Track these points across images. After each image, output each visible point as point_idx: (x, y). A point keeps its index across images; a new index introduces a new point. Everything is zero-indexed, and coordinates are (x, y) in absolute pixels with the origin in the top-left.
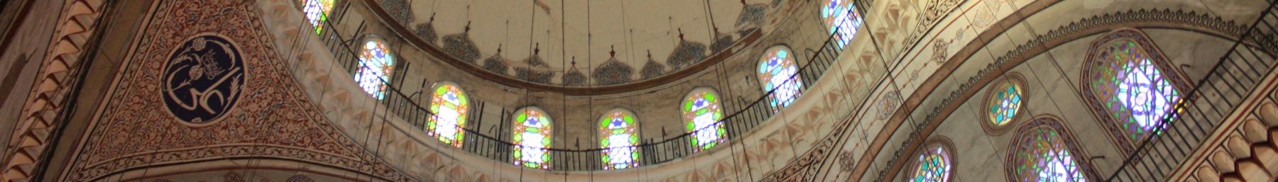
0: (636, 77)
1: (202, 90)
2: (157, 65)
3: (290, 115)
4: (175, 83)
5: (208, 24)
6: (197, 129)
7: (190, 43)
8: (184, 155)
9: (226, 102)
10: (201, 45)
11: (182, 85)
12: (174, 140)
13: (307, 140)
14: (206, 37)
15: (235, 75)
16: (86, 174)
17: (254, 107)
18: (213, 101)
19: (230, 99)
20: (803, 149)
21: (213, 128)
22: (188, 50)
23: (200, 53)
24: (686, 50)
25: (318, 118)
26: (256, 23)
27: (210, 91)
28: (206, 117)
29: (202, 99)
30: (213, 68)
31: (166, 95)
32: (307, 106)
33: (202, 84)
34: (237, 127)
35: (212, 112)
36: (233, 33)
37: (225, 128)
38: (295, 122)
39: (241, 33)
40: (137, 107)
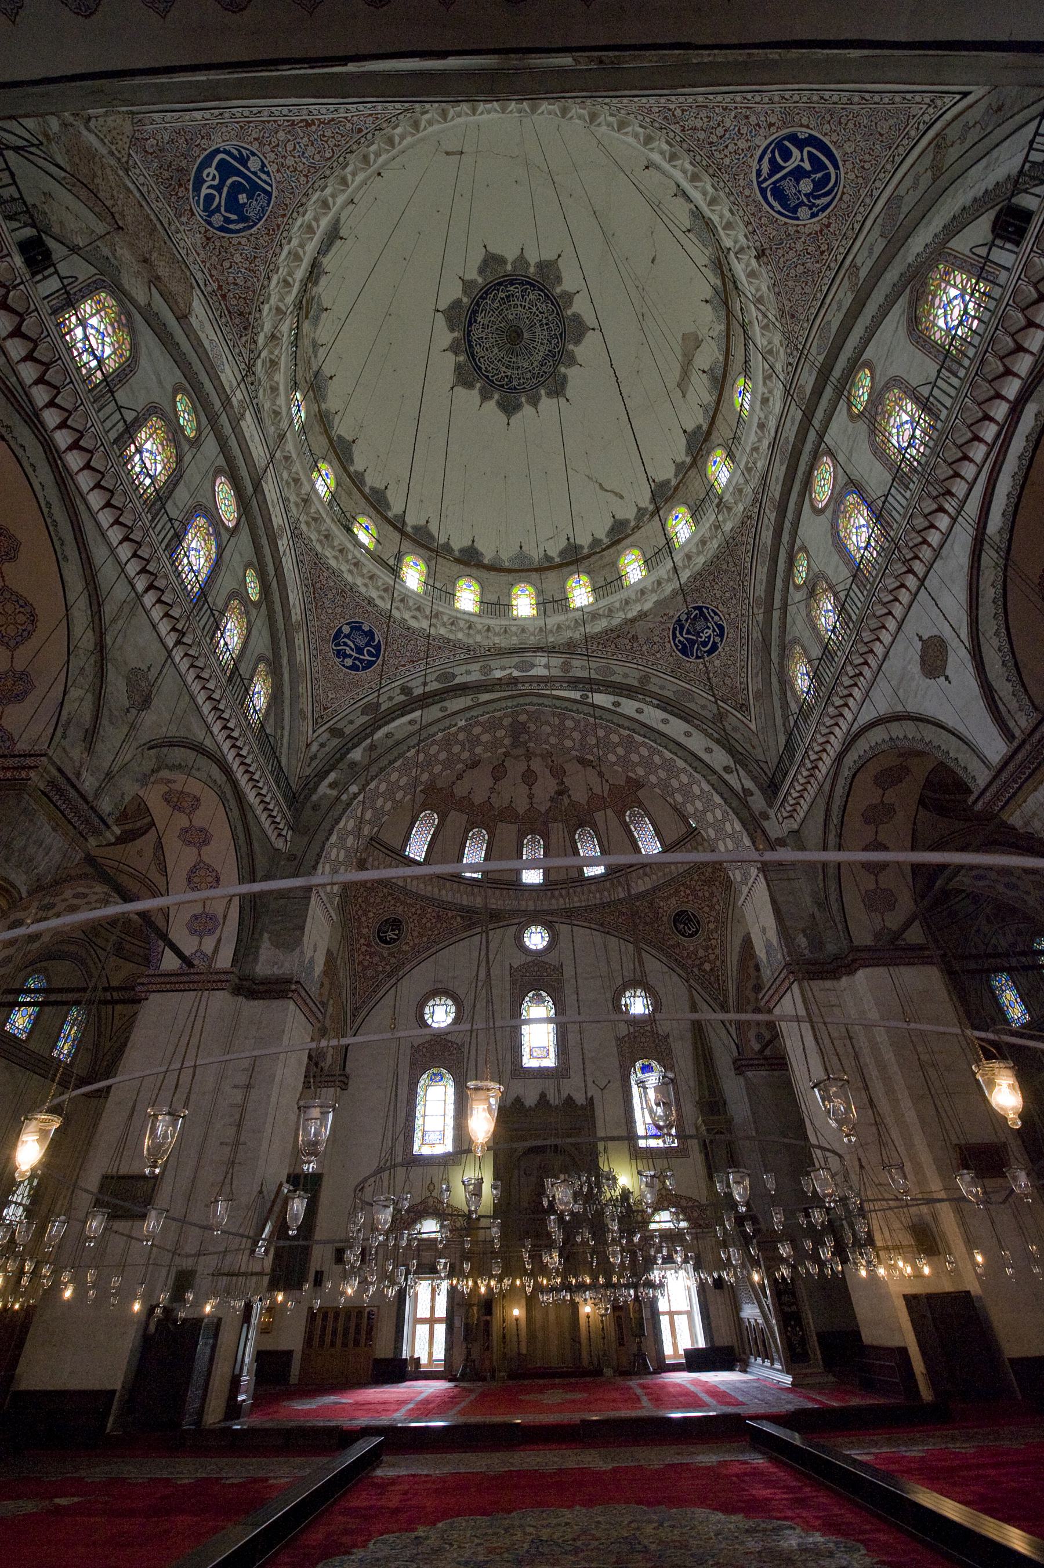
1: (799, 167)
2: (846, 198)
3: (702, 135)
4: (828, 177)
5: (797, 232)
6: (802, 126)
8: (815, 98)
9: (773, 152)
10: (803, 212)
11: (819, 175)
12: (828, 117)
13: (678, 112)
14: (798, 219)
15: (765, 180)
16: (927, 100)
17: (742, 144)
18: (787, 155)
19: (768, 155)
22: (815, 209)
25: (672, 135)
26: (751, 228)
27: (791, 165)
28: (793, 138)
29: (798, 158)
30: (789, 187)
31: (836, 167)
33: (798, 174)
34: (758, 125)
35: (786, 143)
37: (771, 125)
38: (695, 129)
40: (867, 157)
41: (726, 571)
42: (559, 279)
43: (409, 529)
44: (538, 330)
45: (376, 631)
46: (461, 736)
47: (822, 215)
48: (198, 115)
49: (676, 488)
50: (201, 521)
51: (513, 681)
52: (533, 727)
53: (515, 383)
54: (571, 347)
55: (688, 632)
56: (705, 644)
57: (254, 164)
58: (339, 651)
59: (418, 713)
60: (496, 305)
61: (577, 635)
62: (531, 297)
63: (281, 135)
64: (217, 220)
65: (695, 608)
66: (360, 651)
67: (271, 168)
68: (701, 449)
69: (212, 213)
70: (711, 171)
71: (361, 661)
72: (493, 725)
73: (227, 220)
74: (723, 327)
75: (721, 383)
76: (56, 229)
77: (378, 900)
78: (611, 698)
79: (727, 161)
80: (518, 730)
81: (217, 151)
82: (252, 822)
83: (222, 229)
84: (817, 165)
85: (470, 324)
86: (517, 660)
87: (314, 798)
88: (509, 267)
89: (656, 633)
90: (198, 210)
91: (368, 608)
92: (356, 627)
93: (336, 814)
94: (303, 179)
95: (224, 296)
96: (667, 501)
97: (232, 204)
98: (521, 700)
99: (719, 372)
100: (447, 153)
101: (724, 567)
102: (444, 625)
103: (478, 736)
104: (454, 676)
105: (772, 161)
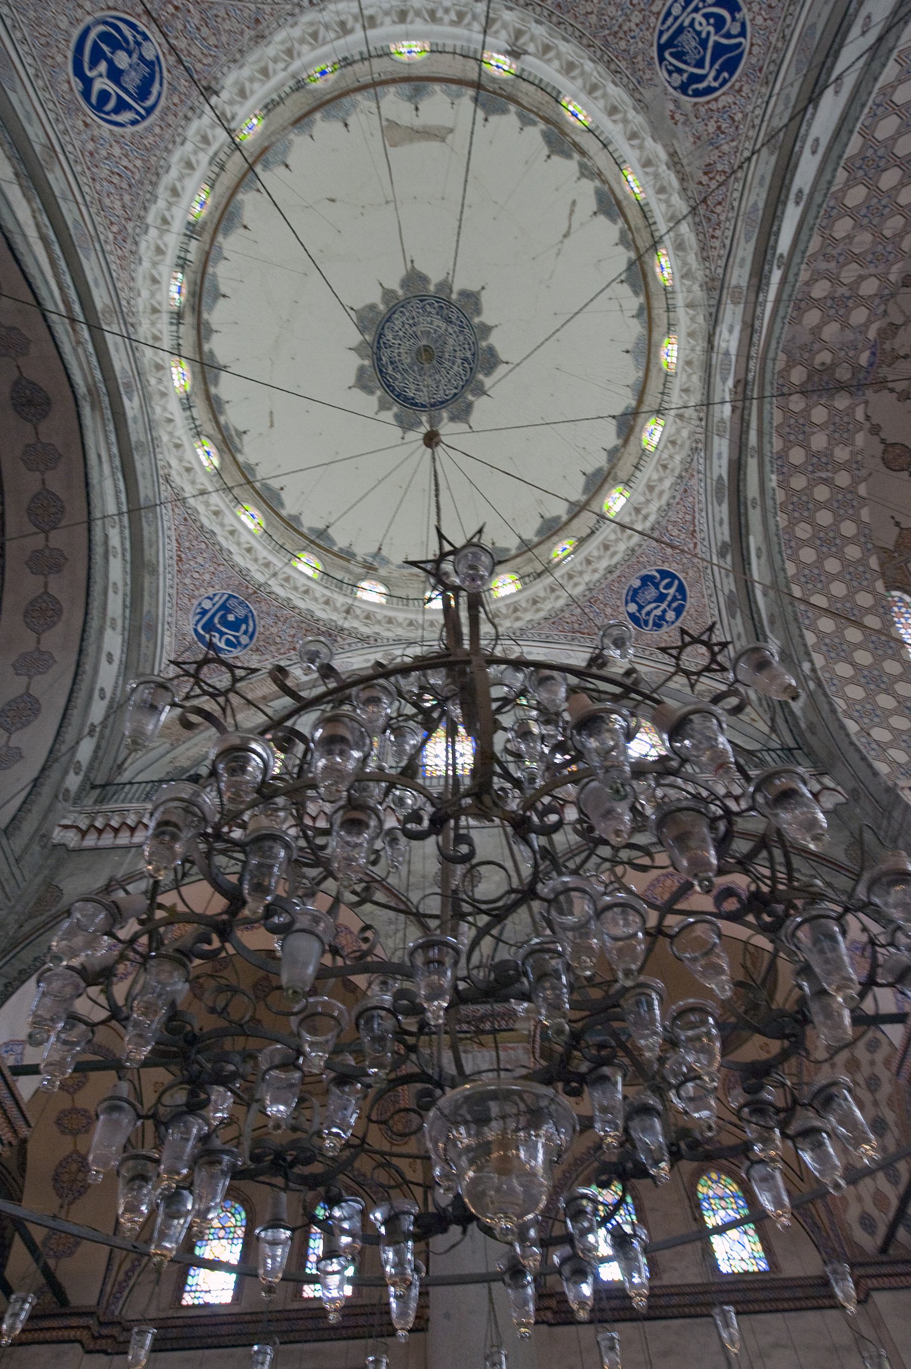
0: (284, 513)
4: (104, 36)
7: (146, 38)
9: (108, 113)
13: (115, 229)
14: (158, 58)
15: (138, 113)
17: (117, 151)
18: (104, 96)
20: (365, 631)
21: (79, 109)
23: (141, 58)
26: (190, 114)
27: (111, 87)
28: (86, 94)
29: (101, 84)
30: (132, 80)
32: (142, 213)
33: (115, 74)
35: (94, 100)
36: (173, 89)
37: (86, 125)
39: (176, 100)
41: (601, 14)
42: (372, 307)
43: (584, 498)
44: (419, 329)
45: (644, 572)
46: (799, 482)
47: (142, 28)
48: (167, 640)
49: (547, 120)
51: (742, 385)
52: (825, 357)
53: (468, 354)
54: (432, 288)
55: (700, 64)
56: (719, 23)
57: (207, 605)
58: (655, 624)
59: (751, 539)
60: (398, 376)
61: (700, 275)
62: (390, 337)
63: (187, 581)
64: (244, 640)
65: (662, 59)
66: (661, 598)
67: (211, 592)
68: (494, 93)
69: (239, 643)
70: (154, 179)
71: (674, 599)
72: (797, 430)
73: (245, 633)
74: (359, 97)
75: (416, 83)
76: (186, 764)
78: (791, 205)
79: (139, 163)
80: (821, 384)
81: (196, 631)
83: (251, 638)
84: (97, 56)
85: (416, 405)
86: (718, 377)
87: (803, 725)
88: (367, 363)
89: (701, 128)
91: (615, 575)
92: (634, 595)
93: (825, 708)
94: (221, 568)
96: (564, 134)
97: (234, 626)
98: (768, 376)
99: (406, 88)
100: (272, 426)
101: (593, 19)
102: (661, 480)
103: (811, 454)
104: (720, 477)
105: (117, 111)
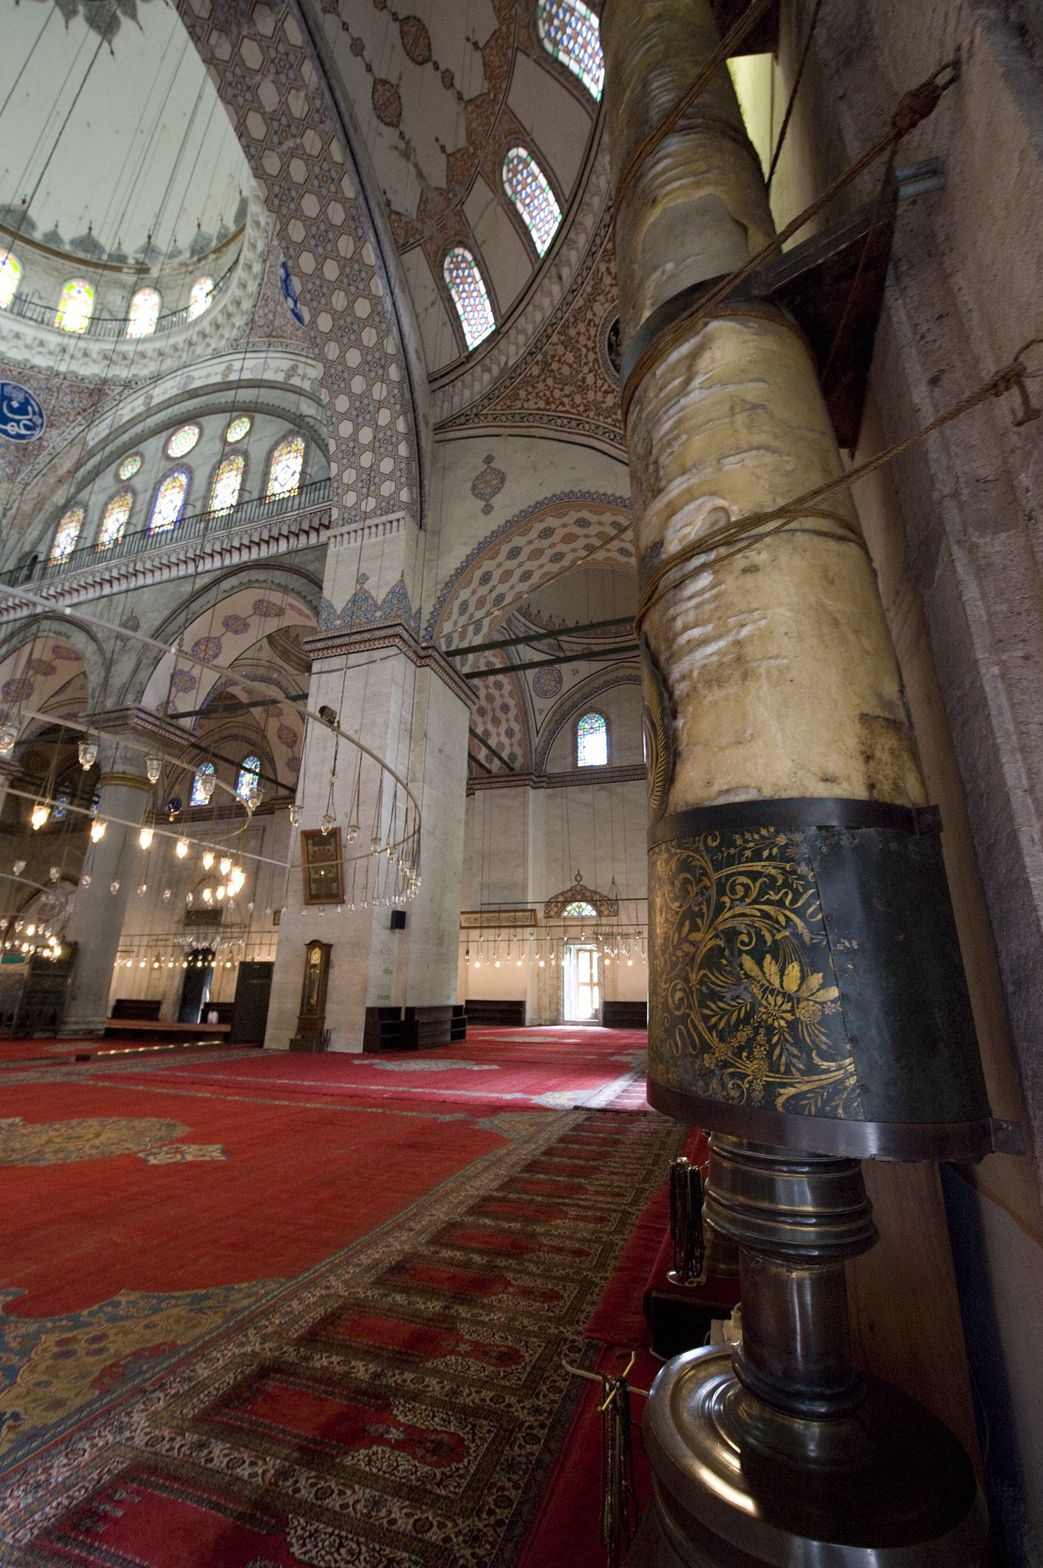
24: (87, 242)
50: (183, 479)
69: (35, 425)
73: (34, 413)
77: (570, 357)
82: (297, 560)
83: (41, 416)
90: (38, 434)
95: (85, 410)
97: (22, 410)
